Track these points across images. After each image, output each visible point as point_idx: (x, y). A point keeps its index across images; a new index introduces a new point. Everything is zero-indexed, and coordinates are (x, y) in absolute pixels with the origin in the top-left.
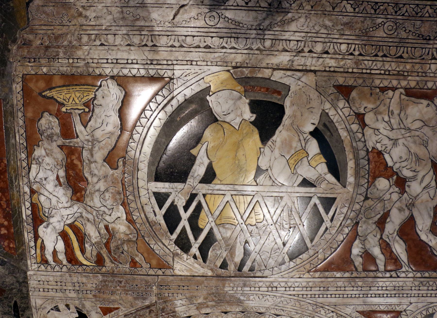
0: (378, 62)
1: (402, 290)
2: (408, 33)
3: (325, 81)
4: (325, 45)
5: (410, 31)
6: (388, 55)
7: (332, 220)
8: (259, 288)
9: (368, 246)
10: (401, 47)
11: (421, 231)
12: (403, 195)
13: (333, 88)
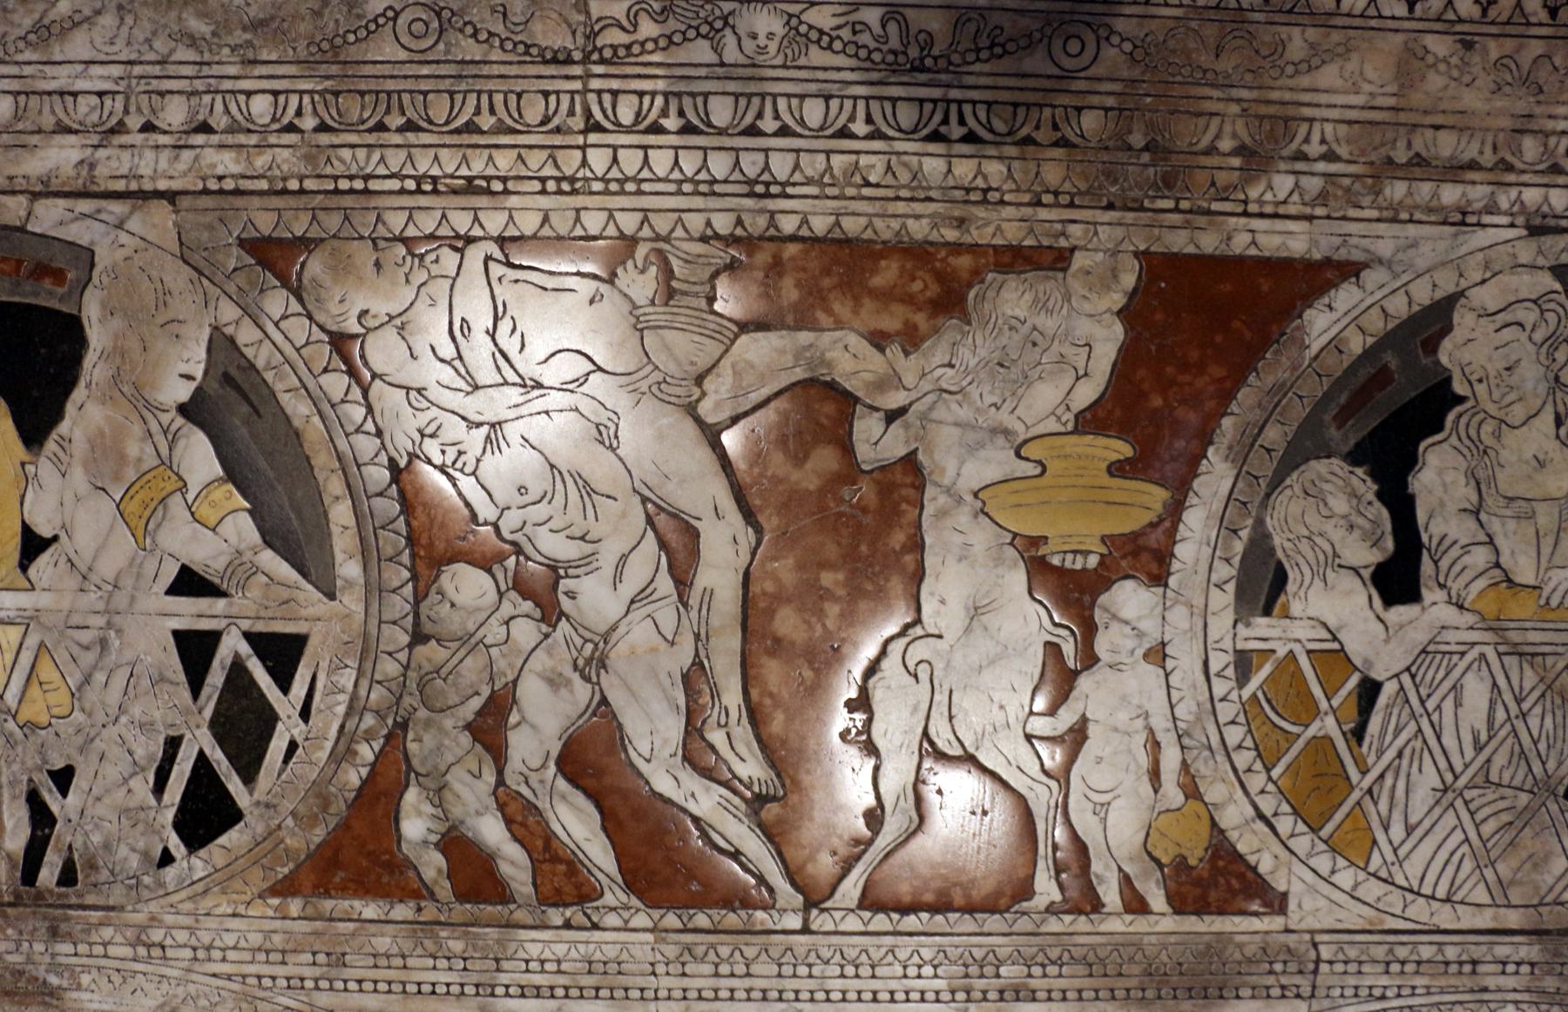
0: (389, 152)
1: (620, 973)
2: (486, 41)
3: (210, 227)
4: (194, 100)
5: (491, 34)
6: (424, 125)
7: (305, 714)
8: (105, 945)
9: (456, 812)
10: (466, 92)
11: (648, 761)
12: (554, 627)
13: (235, 251)
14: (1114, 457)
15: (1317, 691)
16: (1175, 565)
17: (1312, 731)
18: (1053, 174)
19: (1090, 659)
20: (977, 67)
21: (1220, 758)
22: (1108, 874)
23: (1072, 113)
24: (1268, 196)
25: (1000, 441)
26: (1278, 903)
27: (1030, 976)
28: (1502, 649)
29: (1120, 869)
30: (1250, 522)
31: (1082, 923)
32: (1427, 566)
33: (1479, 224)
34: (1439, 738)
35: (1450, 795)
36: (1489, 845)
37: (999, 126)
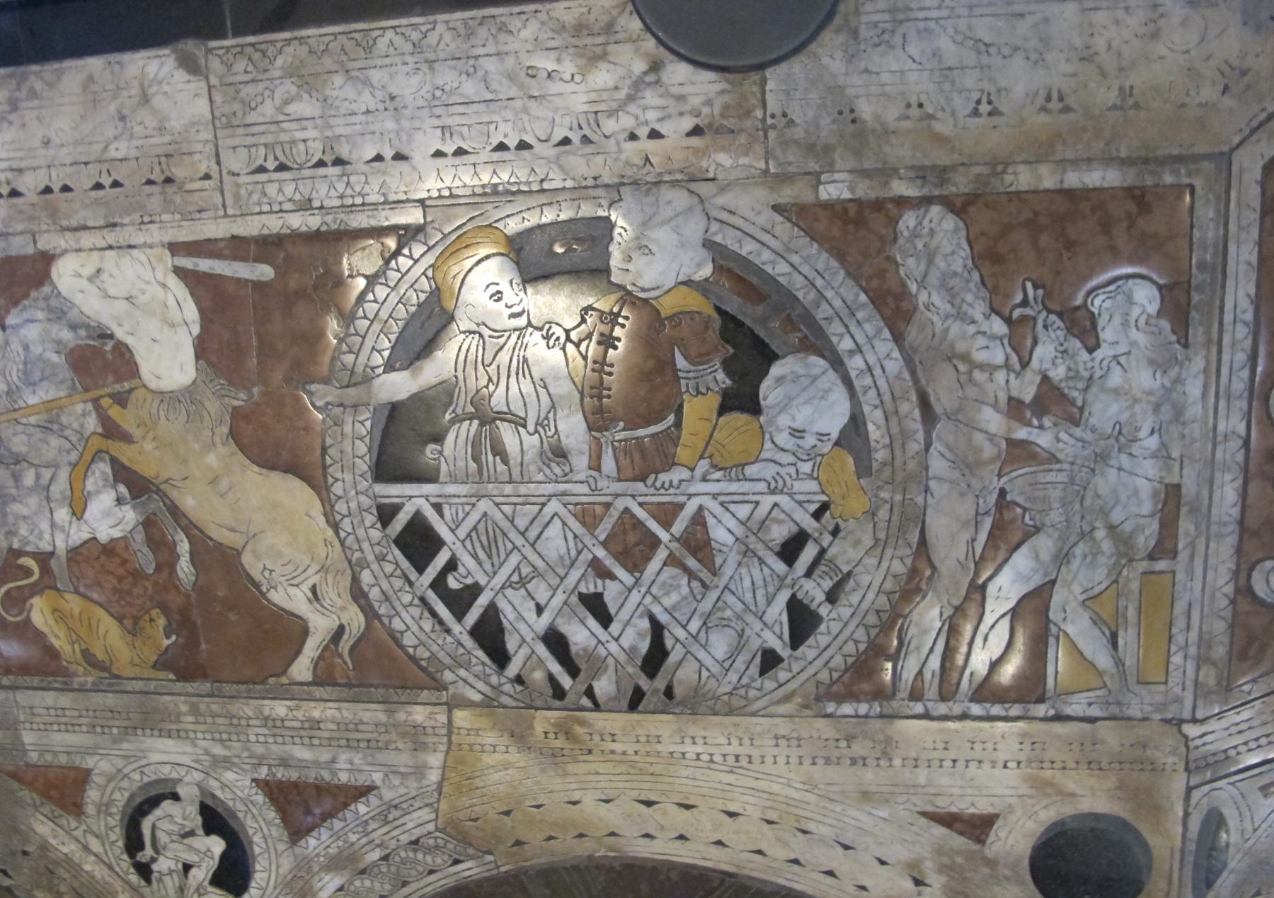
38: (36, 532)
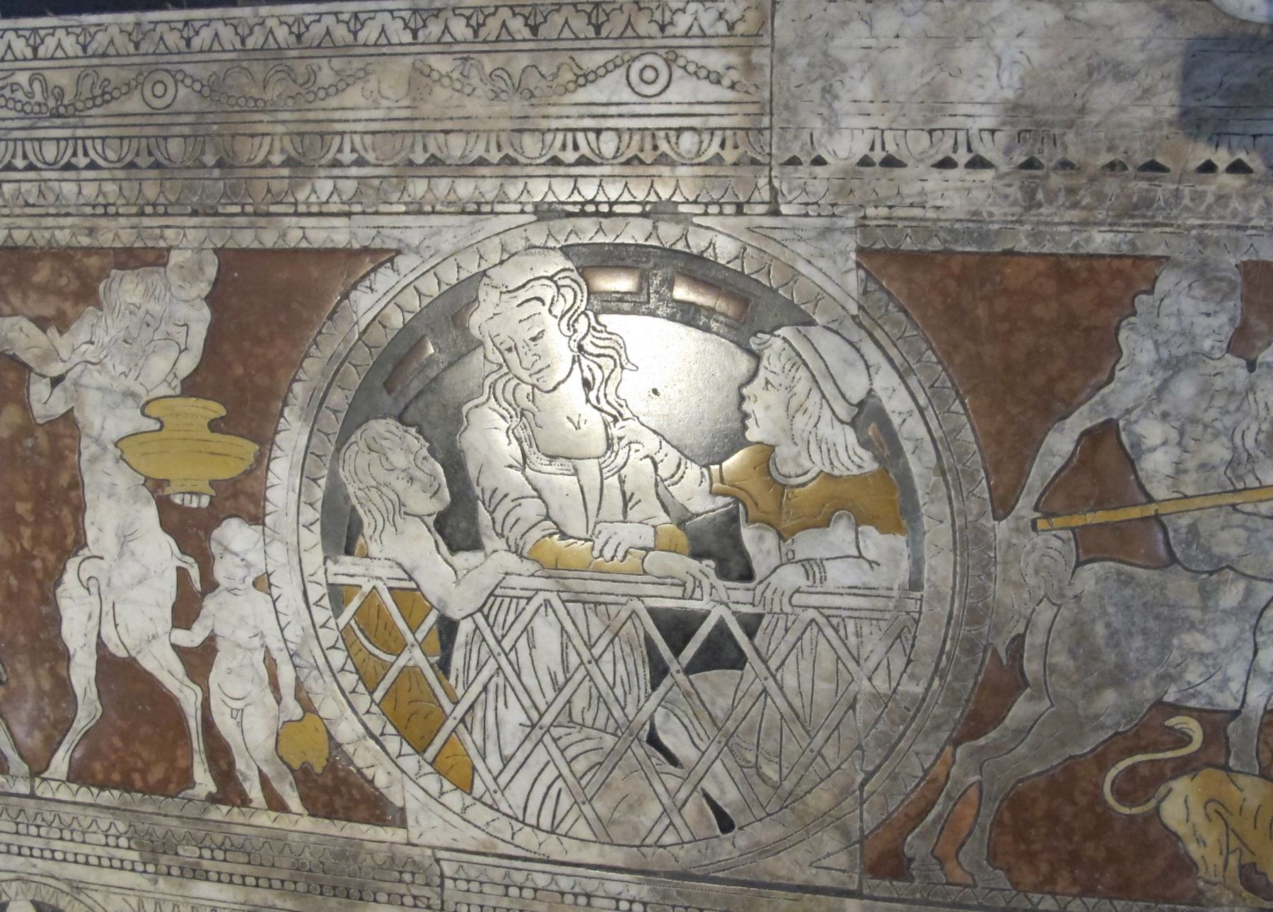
14: (213, 416)
15: (401, 624)
16: (269, 508)
17: (402, 661)
18: (151, 191)
19: (210, 585)
20: (94, 111)
21: (328, 677)
22: (249, 773)
23: (161, 141)
24: (313, 199)
25: (130, 402)
26: (399, 818)
27: (201, 857)
28: (565, 596)
29: (260, 771)
30: (325, 472)
31: (236, 815)
32: (484, 516)
33: (492, 212)
34: (519, 676)
35: (538, 732)
36: (583, 782)
37: (112, 156)
38: (1218, 677)
